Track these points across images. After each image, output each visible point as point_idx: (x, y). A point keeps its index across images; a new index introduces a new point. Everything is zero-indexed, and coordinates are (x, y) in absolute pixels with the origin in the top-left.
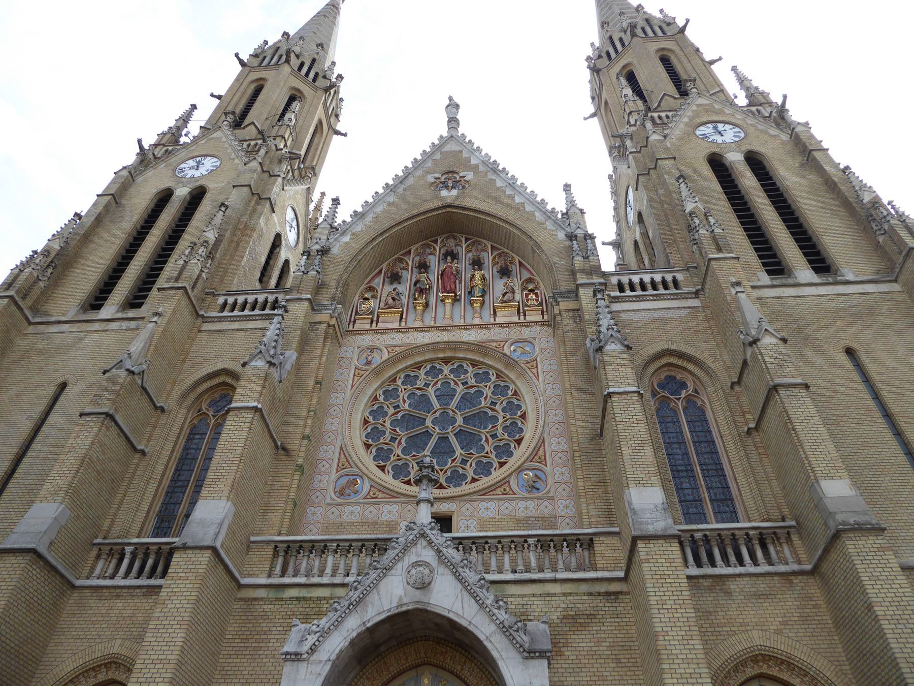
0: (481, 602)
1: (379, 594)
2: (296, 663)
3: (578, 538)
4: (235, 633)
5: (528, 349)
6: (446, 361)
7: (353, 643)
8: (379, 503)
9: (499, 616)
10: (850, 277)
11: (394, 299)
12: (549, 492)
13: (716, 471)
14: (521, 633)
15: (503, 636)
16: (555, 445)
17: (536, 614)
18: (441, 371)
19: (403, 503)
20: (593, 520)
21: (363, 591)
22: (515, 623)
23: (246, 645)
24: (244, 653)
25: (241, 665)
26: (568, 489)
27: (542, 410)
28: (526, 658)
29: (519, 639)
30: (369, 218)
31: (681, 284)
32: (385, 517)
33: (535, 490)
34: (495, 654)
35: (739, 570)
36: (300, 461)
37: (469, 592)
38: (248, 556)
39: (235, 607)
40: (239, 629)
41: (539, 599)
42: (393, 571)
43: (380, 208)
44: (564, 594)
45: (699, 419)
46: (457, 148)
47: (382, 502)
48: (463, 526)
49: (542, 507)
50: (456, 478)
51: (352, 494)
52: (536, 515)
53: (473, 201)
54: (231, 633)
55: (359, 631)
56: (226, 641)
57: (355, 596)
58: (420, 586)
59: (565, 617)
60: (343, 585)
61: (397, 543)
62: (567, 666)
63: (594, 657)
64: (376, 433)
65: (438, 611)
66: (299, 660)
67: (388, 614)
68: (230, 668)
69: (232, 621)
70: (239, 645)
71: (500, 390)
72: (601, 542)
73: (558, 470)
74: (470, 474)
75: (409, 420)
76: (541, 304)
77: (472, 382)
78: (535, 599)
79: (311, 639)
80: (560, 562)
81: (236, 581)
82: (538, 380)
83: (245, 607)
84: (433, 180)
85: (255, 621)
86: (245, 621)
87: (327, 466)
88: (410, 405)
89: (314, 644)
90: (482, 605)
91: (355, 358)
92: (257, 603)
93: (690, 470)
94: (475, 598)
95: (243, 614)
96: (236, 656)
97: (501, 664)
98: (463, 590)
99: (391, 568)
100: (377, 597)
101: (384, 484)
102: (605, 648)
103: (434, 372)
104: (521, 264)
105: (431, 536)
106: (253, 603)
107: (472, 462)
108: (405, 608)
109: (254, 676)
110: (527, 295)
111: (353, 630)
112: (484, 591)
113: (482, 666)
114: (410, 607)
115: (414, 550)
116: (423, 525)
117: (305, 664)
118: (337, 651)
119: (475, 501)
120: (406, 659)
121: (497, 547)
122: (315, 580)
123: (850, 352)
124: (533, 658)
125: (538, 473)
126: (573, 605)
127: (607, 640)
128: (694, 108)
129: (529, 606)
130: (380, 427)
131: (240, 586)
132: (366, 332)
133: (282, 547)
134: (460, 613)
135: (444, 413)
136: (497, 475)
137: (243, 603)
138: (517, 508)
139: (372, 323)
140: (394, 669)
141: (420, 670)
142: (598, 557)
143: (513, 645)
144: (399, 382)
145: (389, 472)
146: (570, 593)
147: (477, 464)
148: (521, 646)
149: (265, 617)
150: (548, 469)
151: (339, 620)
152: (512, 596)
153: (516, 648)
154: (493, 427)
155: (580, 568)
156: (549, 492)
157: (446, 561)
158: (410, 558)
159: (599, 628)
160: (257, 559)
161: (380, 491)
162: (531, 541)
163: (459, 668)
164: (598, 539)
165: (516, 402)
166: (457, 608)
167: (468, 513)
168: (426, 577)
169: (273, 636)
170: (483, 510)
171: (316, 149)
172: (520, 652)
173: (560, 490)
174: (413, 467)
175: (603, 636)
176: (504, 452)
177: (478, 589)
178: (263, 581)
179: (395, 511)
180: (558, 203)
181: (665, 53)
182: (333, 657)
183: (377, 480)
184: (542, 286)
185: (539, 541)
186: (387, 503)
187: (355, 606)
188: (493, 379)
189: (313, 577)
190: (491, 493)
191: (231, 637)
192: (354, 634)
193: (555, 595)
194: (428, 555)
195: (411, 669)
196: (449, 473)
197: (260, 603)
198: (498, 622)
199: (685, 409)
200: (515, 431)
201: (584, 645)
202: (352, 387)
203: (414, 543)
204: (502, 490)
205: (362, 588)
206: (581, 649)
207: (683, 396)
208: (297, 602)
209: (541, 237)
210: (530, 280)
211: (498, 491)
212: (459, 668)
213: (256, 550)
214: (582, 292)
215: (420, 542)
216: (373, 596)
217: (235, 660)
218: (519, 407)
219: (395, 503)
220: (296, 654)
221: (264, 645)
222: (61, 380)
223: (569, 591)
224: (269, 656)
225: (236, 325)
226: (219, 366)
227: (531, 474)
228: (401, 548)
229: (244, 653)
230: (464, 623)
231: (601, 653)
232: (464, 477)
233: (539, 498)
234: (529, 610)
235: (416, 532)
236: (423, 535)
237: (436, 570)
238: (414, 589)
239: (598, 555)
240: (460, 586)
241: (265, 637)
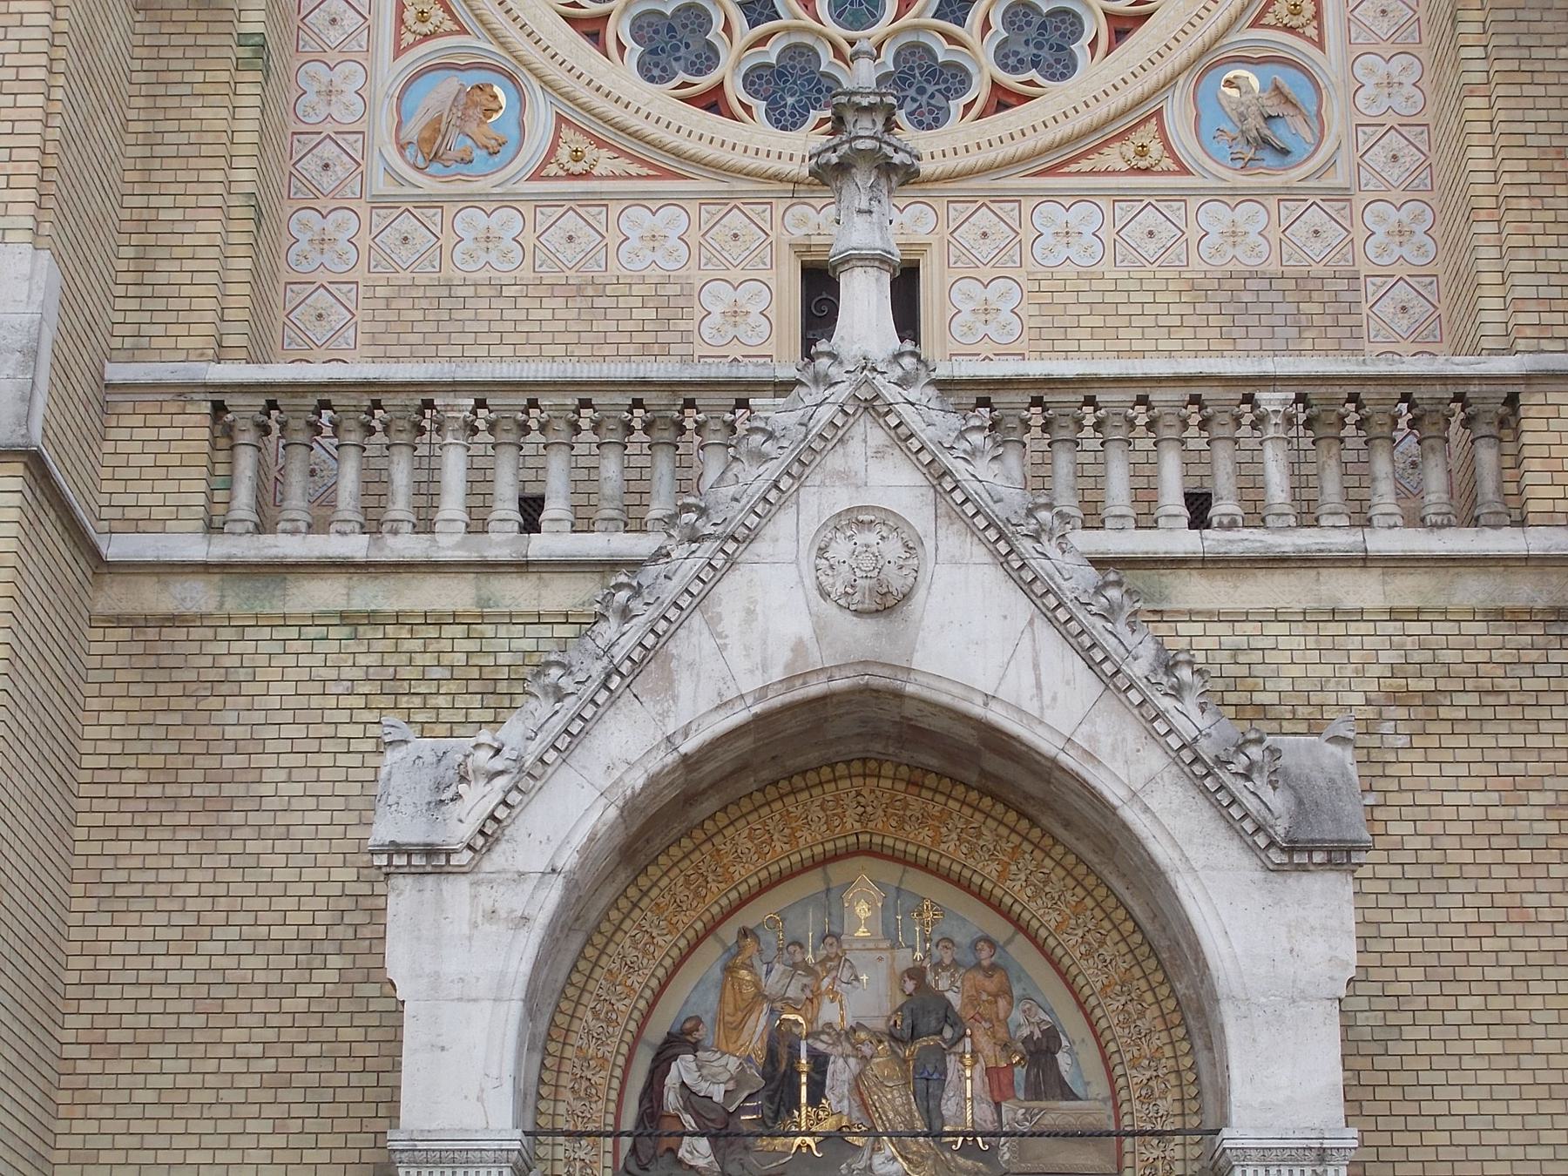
0: (1108, 668)
1: (716, 635)
2: (430, 880)
3: (1460, 392)
4: (117, 748)
7: (629, 809)
8: (601, 200)
9: (1179, 722)
12: (1331, 163)
14: (1260, 782)
15: (1193, 792)
17: (1285, 685)
19: (705, 200)
20: (1522, 318)
21: (655, 621)
22: (1240, 749)
23: (171, 790)
24: (168, 819)
25: (166, 862)
26: (1410, 157)
28: (1279, 869)
29: (1251, 804)
32: (634, 261)
33: (1269, 158)
34: (1161, 851)
36: (253, 23)
37: (1061, 628)
38: (108, 447)
39: (96, 648)
40: (131, 733)
41: (1298, 628)
42: (760, 547)
44: (1394, 614)
47: (618, 197)
48: (967, 308)
49: (1300, 231)
51: (479, 154)
52: (1273, 267)
54: (103, 747)
55: (654, 765)
56: (85, 776)
57: (628, 642)
58: (869, 605)
59: (1396, 698)
60: (523, 566)
61: (771, 436)
62: (1396, 871)
63: (1496, 842)
65: (945, 699)
66: (439, 872)
67: (757, 709)
68: (122, 876)
69: (94, 704)
70: (143, 791)
72: (1549, 411)
73: (1372, 68)
74: (984, 69)
78: (1282, 628)
79: (478, 800)
80: (1385, 488)
81: (94, 552)
83: (138, 648)
85: (188, 703)
86: (148, 703)
89: (492, 817)
90: (1112, 681)
92: (181, 634)
94: (1085, 654)
95: (134, 676)
96: (139, 834)
97: (1186, 888)
98: (1040, 623)
99: (750, 537)
100: (709, 645)
101: (615, 112)
102: (1538, 813)
105: (907, 412)
106: (168, 633)
108: (816, 688)
109: (223, 904)
111: (631, 765)
112: (1121, 628)
113: (1071, 859)
114: (839, 684)
115: (835, 461)
116: (867, 365)
117: (463, 883)
118: (580, 839)
119: (1015, 198)
120: (792, 839)
121: (1131, 423)
122: (405, 546)
124: (1302, 868)
125: (1285, 77)
126: (1427, 656)
127: (1549, 783)
129: (1256, 657)
131: (101, 567)
133: (244, 408)
134: (1032, 707)
137: (124, 633)
138: (1193, 234)
140: (746, 873)
141: (837, 871)
142: (1535, 474)
143: (1230, 823)
145: (621, 47)
146: (1419, 611)
147: (1010, 20)
148: (1259, 829)
149: (224, 689)
150: (1329, 64)
151: (575, 729)
152: (1191, 615)
153: (1240, 834)
156: (1331, 163)
157: (970, 509)
159: (1518, 741)
160: (149, 460)
161: (601, 144)
162: (1270, 400)
163: (992, 869)
164: (1539, 398)
166: (1019, 687)
167: (985, 250)
168: (891, 573)
169: (270, 761)
170: (1048, 239)
172: (1253, 848)
173: (1378, 157)
174: (727, 28)
175: (1533, 768)
177: (1099, 622)
178: (196, 548)
179: (674, 235)
182: (568, 860)
183: (585, 95)
185: (1300, 398)
186: (639, 199)
187: (629, 680)
189: (395, 532)
190: (1085, 165)
191: (103, 762)
192: (638, 780)
193: (1360, 614)
195: (805, 869)
196: (888, 55)
197: (196, 633)
198: (1174, 742)
201: (1463, 798)
203: (835, 435)
204: (1130, 150)
205: (653, 612)
206: (1449, 813)
208: (345, 631)
211: (1113, 157)
212: (992, 869)
213: (138, 420)
215: (858, 431)
216: (692, 643)
217: (139, 847)
219: (672, 200)
220: (430, 851)
221: (240, 790)
223: (1413, 603)
224: (272, 832)
227: (1255, 83)
228: (786, 457)
229: (168, 819)
230: (1045, 743)
231: (1522, 827)
232: (956, 79)
233: (1287, 194)
234: (1259, 670)
235: (842, 392)
236: (872, 406)
237: (929, 544)
238: (848, 616)
239: (1535, 464)
240: (1022, 607)
241: (239, 761)
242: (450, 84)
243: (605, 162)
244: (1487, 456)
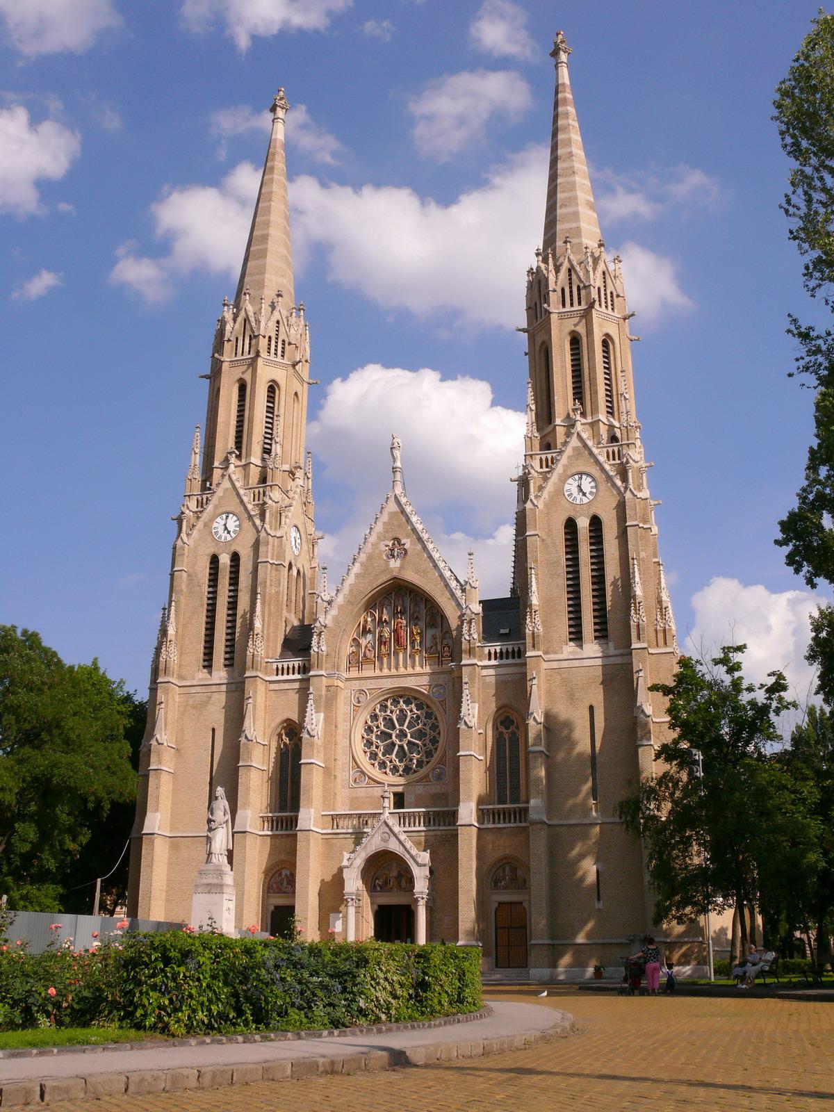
5: (442, 691)
35: (508, 825)
53: (411, 576)
64: (369, 743)
93: (505, 773)
103: (396, 702)
150: (446, 769)
155: (450, 825)
171: (297, 426)
199: (510, 738)
218: (438, 727)
222: (211, 727)
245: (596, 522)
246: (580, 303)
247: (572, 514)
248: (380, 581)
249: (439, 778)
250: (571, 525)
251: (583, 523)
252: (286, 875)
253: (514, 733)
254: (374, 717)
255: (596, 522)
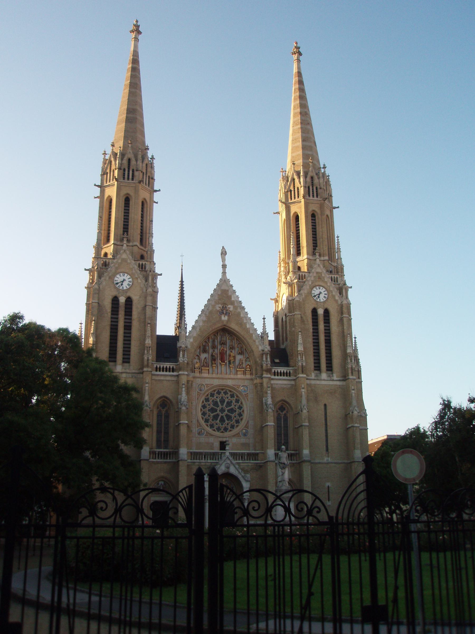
6: (222, 389)
10: (335, 378)
11: (206, 363)
13: (286, 435)
16: (251, 423)
18: (220, 393)
27: (249, 411)
30: (198, 330)
31: (291, 374)
43: (201, 324)
45: (286, 420)
46: (227, 288)
50: (226, 429)
53: (233, 326)
64: (204, 414)
71: (237, 401)
75: (212, 410)
76: (250, 371)
77: (230, 398)
82: (248, 400)
84: (218, 309)
87: (194, 426)
88: (213, 404)
90: (239, 472)
91: (197, 388)
97: (242, 482)
104: (245, 349)
107: (230, 425)
110: (247, 366)
123: (325, 405)
128: (315, 275)
130: (205, 412)
132: (199, 378)
135: (222, 408)
136: (235, 431)
139: (200, 373)
142: (259, 458)
144: (209, 396)
150: (249, 430)
154: (235, 414)
155: (255, 460)
158: (225, 462)
165: (241, 406)
176: (237, 422)
180: (260, 331)
181: (314, 212)
184: (251, 362)
188: (235, 397)
194: (229, 462)
200: (240, 415)
202: (197, 399)
207: (283, 413)
209: (254, 348)
210: (248, 358)
214: (264, 380)
225: (162, 378)
226: (162, 395)
232: (228, 429)
242: (200, 430)
243: (209, 435)
244: (256, 457)
245: (327, 312)
246: (317, 196)
247: (316, 306)
248: (216, 326)
249: (245, 435)
250: (314, 311)
251: (321, 312)
252: (161, 484)
253: (285, 415)
254: (207, 400)
255: (327, 312)
